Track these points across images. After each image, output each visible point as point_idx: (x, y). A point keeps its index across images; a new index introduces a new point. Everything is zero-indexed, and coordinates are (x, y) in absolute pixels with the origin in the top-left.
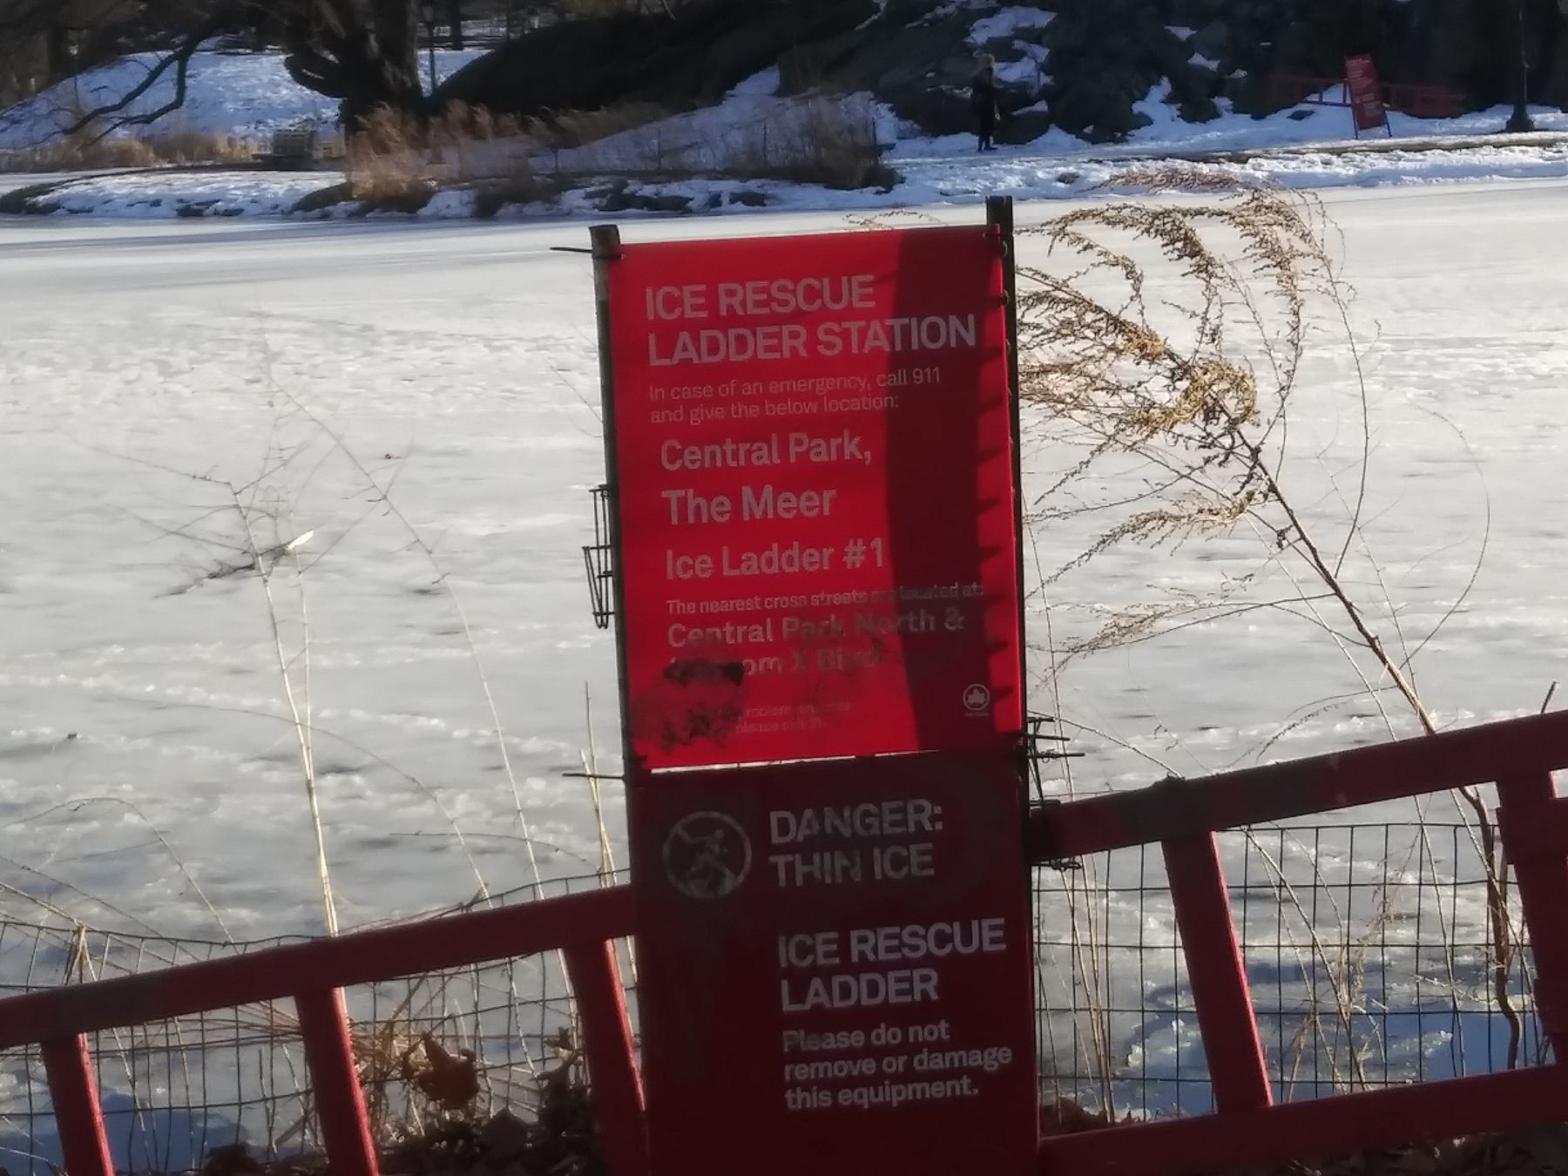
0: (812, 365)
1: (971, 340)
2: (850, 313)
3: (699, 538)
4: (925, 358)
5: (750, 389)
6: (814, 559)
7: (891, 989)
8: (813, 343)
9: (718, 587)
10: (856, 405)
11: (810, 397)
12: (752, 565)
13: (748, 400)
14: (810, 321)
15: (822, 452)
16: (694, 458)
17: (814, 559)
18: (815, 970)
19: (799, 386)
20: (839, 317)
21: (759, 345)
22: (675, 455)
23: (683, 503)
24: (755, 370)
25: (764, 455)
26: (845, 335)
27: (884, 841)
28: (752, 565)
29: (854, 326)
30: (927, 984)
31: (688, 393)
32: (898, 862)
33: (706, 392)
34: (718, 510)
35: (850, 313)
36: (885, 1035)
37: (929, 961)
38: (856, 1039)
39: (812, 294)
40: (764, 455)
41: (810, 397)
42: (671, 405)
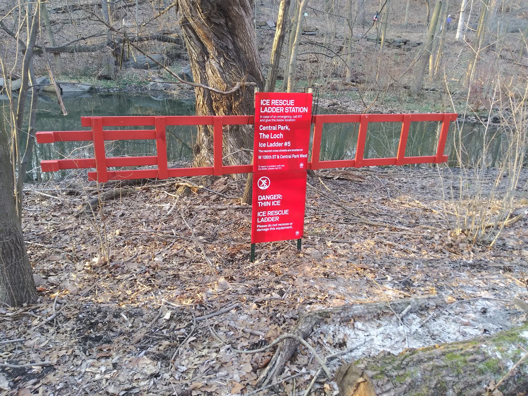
0: (284, 114)
1: (307, 111)
2: (290, 106)
3: (265, 141)
4: (300, 114)
5: (274, 117)
6: (280, 145)
7: (272, 219)
8: (284, 110)
9: (266, 148)
10: (290, 120)
11: (283, 119)
12: (271, 145)
13: (274, 119)
14: (284, 107)
15: (283, 128)
16: (264, 128)
17: (280, 145)
18: (262, 217)
19: (282, 117)
20: (288, 106)
21: (277, 110)
22: (262, 128)
23: (262, 135)
24: (276, 114)
25: (274, 128)
26: (289, 109)
27: (274, 200)
28: (271, 145)
29: (290, 108)
30: (277, 219)
31: (266, 117)
32: (276, 203)
33: (268, 117)
34: (267, 136)
35: (290, 106)
36: (269, 225)
37: (278, 215)
38: (266, 226)
39: (285, 103)
40: (274, 128)
41: (283, 119)
42: (263, 119)
